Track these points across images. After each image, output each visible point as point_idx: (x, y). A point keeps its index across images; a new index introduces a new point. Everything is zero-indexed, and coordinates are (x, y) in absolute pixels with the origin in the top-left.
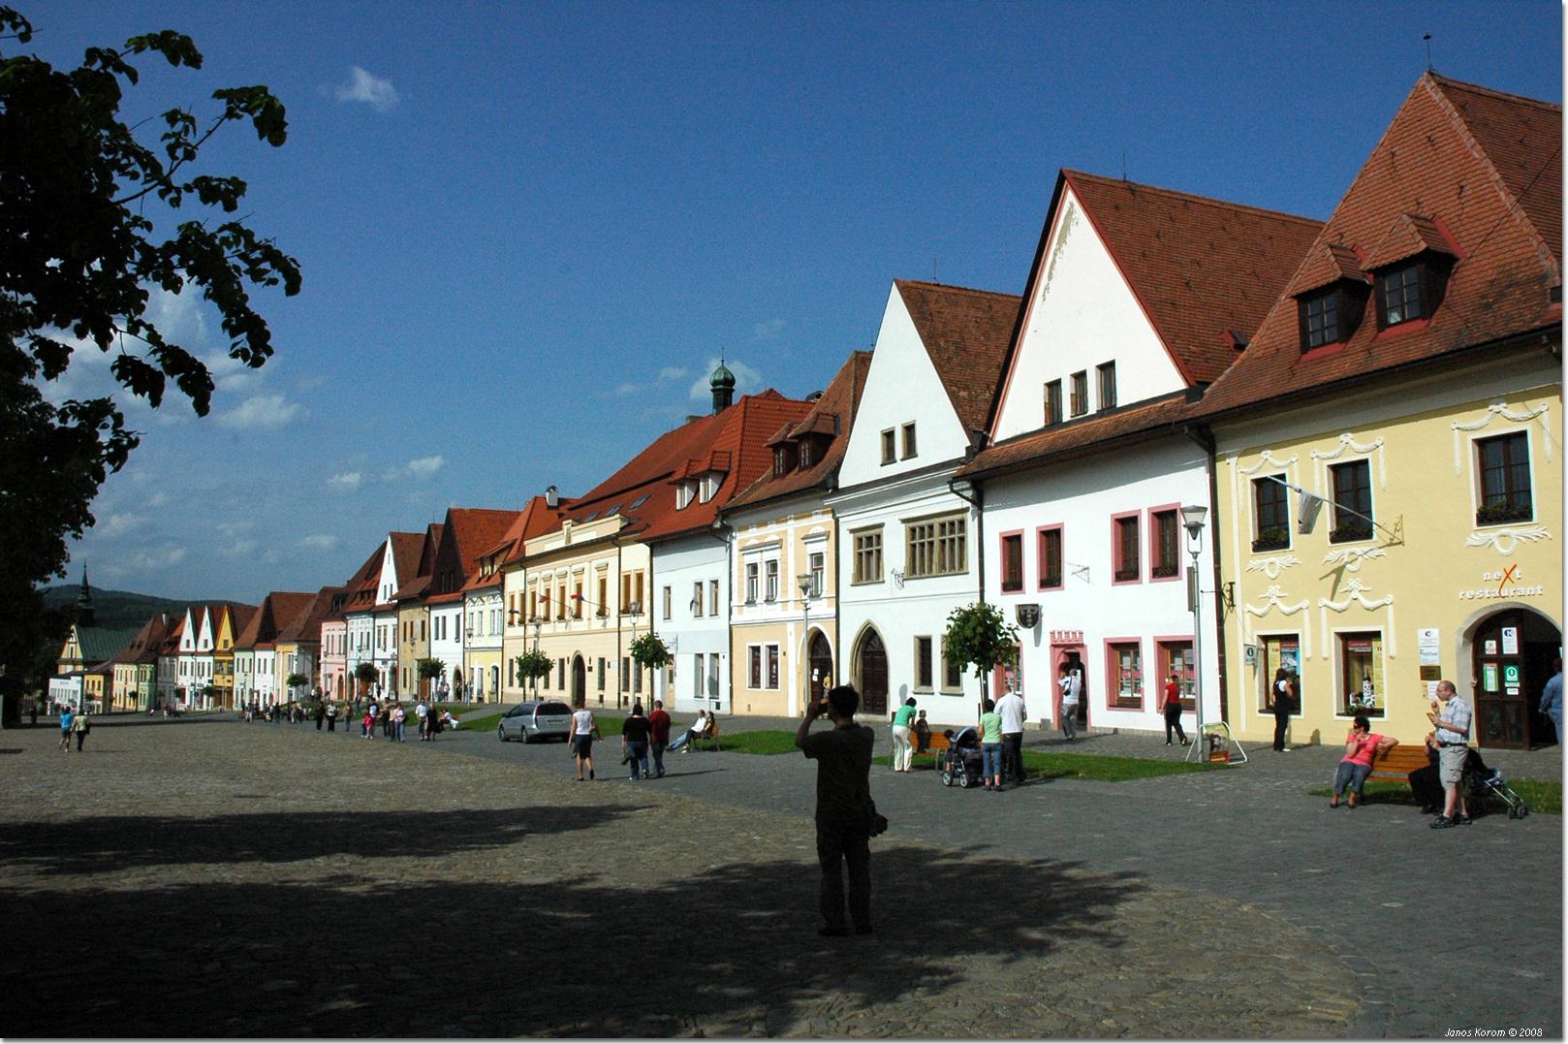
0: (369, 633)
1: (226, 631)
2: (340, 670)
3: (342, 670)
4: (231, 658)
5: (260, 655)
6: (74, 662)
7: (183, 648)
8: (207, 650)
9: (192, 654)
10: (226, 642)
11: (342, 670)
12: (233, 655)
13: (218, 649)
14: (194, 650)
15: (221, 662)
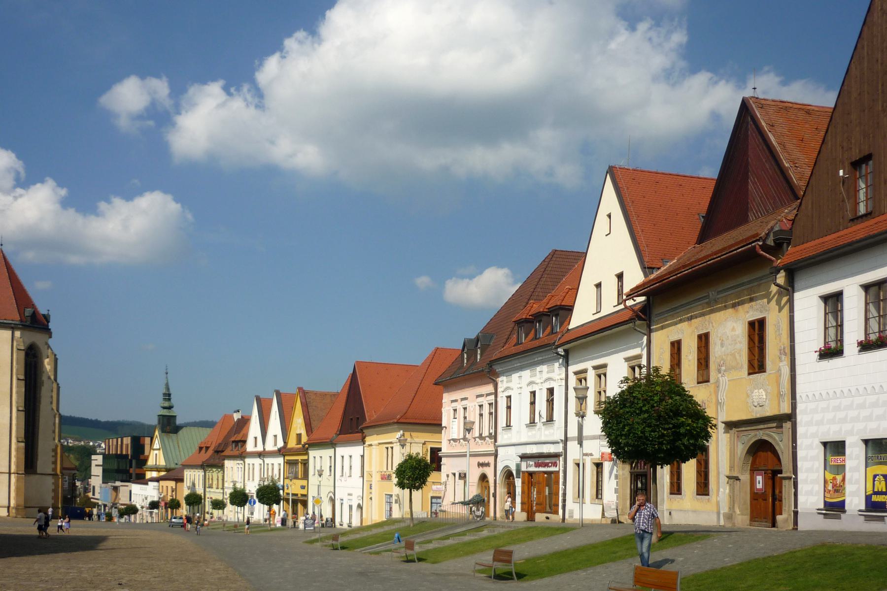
0: (551, 391)
1: (298, 425)
2: (481, 465)
3: (488, 465)
4: (305, 457)
5: (341, 451)
6: (158, 469)
7: (250, 447)
8: (276, 449)
9: (261, 455)
10: (299, 436)
11: (488, 465)
12: (307, 454)
13: (289, 446)
14: (262, 449)
15: (295, 463)
